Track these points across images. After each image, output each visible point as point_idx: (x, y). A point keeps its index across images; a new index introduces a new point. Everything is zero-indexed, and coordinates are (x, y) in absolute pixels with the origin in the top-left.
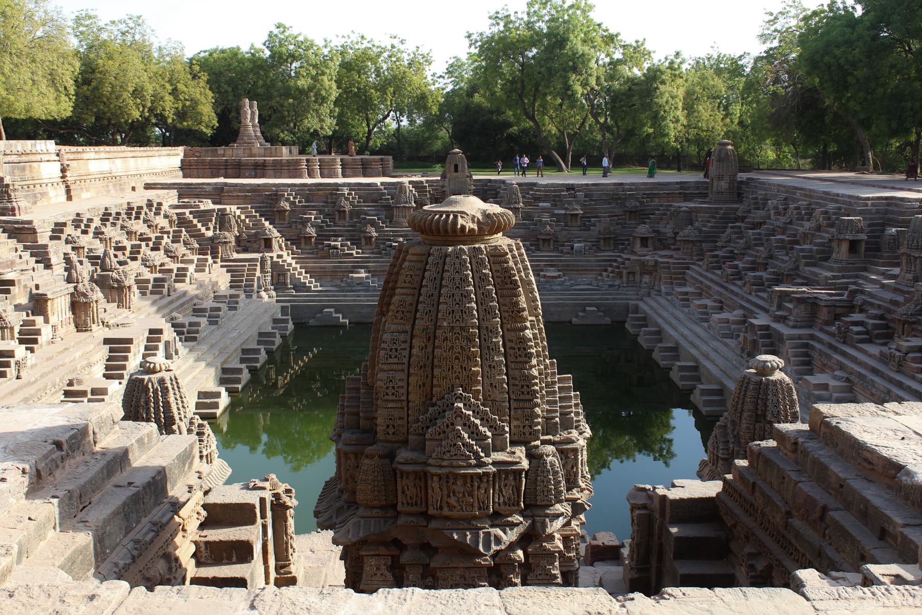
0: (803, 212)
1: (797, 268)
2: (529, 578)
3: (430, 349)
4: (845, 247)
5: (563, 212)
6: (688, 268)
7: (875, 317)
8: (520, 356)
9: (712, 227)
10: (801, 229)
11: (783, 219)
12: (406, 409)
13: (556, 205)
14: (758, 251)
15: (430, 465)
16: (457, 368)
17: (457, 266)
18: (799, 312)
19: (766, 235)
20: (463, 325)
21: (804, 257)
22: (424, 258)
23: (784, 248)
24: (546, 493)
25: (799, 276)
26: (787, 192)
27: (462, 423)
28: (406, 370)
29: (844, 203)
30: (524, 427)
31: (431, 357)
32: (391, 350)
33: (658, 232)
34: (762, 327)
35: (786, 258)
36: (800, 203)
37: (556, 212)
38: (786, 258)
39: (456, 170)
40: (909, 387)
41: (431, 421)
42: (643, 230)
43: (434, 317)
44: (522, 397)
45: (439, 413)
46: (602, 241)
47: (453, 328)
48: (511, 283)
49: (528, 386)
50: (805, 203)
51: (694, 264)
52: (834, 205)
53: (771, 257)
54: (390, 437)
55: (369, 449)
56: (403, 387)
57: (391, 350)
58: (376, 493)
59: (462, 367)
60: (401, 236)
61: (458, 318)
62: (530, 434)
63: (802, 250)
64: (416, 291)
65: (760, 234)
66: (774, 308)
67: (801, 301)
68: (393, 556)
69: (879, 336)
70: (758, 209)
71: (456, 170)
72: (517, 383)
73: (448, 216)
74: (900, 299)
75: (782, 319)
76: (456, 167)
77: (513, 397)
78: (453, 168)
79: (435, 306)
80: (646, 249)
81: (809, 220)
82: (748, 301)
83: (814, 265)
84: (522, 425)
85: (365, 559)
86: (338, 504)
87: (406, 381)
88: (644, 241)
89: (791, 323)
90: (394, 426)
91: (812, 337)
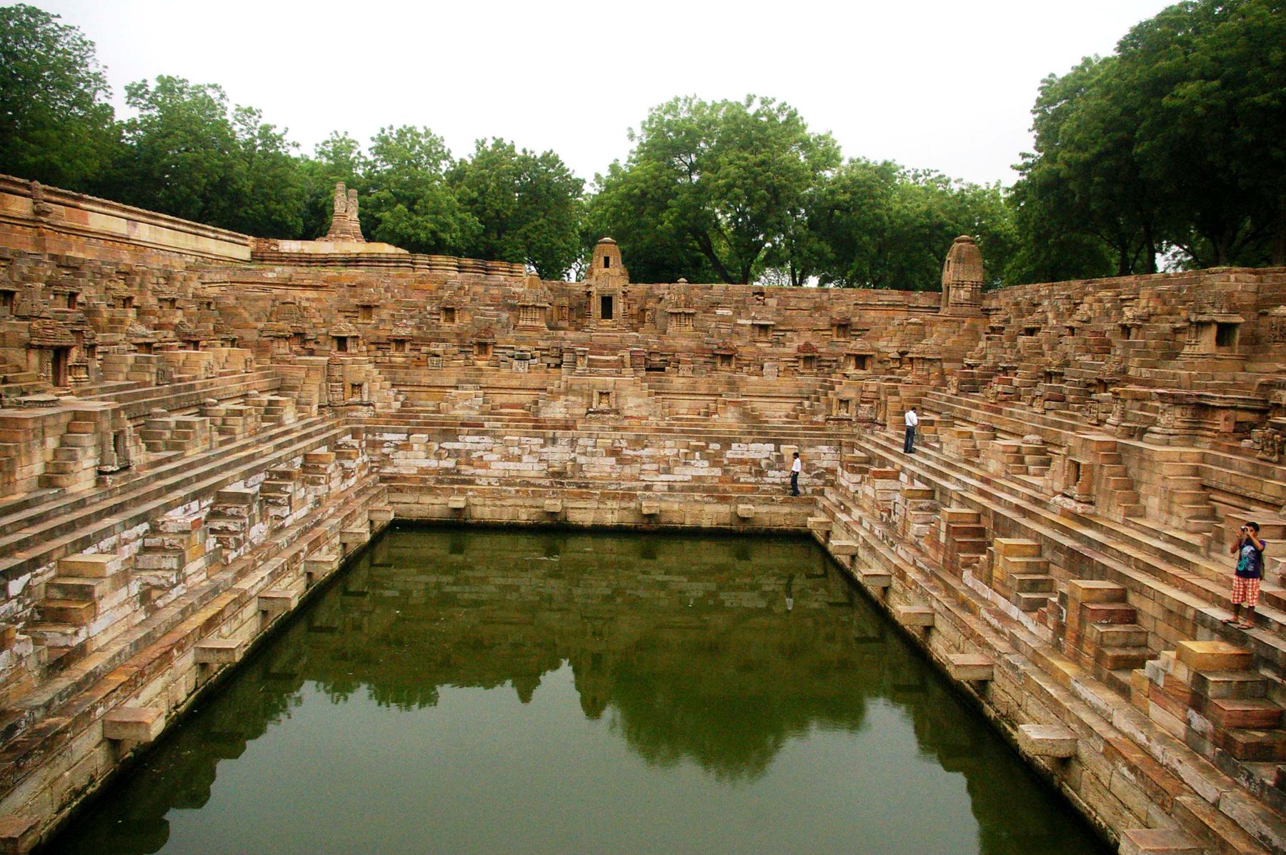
1: (1125, 371)
4: (1209, 336)
5: (750, 322)
37: (739, 322)
39: (607, 265)
42: (857, 345)
46: (801, 362)
53: (1067, 364)
71: (607, 265)
76: (607, 260)
80: (862, 372)
88: (861, 361)
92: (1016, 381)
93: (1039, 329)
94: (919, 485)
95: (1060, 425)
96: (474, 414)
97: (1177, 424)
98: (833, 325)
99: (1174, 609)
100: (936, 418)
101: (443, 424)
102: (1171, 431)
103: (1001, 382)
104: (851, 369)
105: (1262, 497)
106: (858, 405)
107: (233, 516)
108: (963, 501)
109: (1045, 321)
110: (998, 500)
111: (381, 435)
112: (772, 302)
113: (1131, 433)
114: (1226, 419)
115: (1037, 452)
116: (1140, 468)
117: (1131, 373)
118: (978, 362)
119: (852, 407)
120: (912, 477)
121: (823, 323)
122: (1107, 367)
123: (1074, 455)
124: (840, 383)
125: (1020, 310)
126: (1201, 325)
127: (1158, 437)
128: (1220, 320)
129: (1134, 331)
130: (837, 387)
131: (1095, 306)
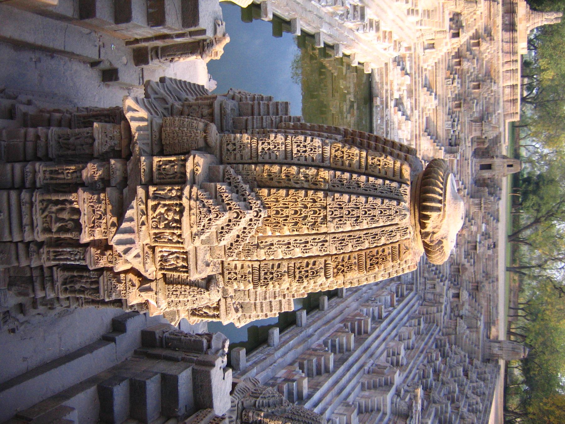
0: (474, 407)
1: (434, 402)
2: (109, 273)
3: (306, 185)
5: (478, 240)
8: (300, 272)
9: (466, 342)
10: (462, 406)
11: (469, 392)
12: (250, 161)
13: (483, 235)
14: (448, 373)
15: (191, 188)
16: (286, 212)
17: (388, 212)
18: (403, 406)
19: (459, 380)
20: (329, 219)
21: (442, 408)
22: (397, 178)
23: (449, 393)
24: (175, 293)
25: (429, 404)
26: (489, 394)
27: (231, 218)
28: (285, 161)
30: (236, 273)
31: (297, 186)
32: (305, 146)
33: (463, 305)
35: (442, 394)
37: (478, 236)
38: (442, 394)
41: (236, 187)
43: (337, 189)
44: (262, 273)
45: (243, 195)
46: (457, 267)
47: (325, 208)
48: (371, 265)
49: (272, 278)
50: (481, 408)
53: (443, 383)
54: (225, 146)
55: (213, 128)
56: (270, 158)
57: (305, 146)
58: (171, 135)
59: (288, 216)
60: (461, 128)
61: (335, 213)
62: (229, 279)
63: (447, 406)
64: (364, 170)
66: (406, 387)
67: (410, 407)
68: (120, 151)
70: (478, 374)
72: (275, 269)
73: (440, 202)
75: (398, 393)
77: (262, 264)
78: (511, 163)
79: (347, 190)
80: (451, 296)
81: (469, 411)
82: (412, 368)
83: (436, 415)
84: (237, 271)
85: (118, 126)
86: (170, 100)
87: (276, 161)
88: (457, 296)
89: (395, 400)
90: (234, 150)
91: (385, 414)
96: (422, 105)
98: (478, 283)
101: (416, 90)
104: (452, 292)
106: (433, 293)
107: (354, 15)
111: (409, 60)
112: (490, 252)
115: (398, 362)
119: (432, 290)
121: (479, 277)
124: (444, 285)
125: (481, 374)
130: (442, 283)
131: (475, 401)
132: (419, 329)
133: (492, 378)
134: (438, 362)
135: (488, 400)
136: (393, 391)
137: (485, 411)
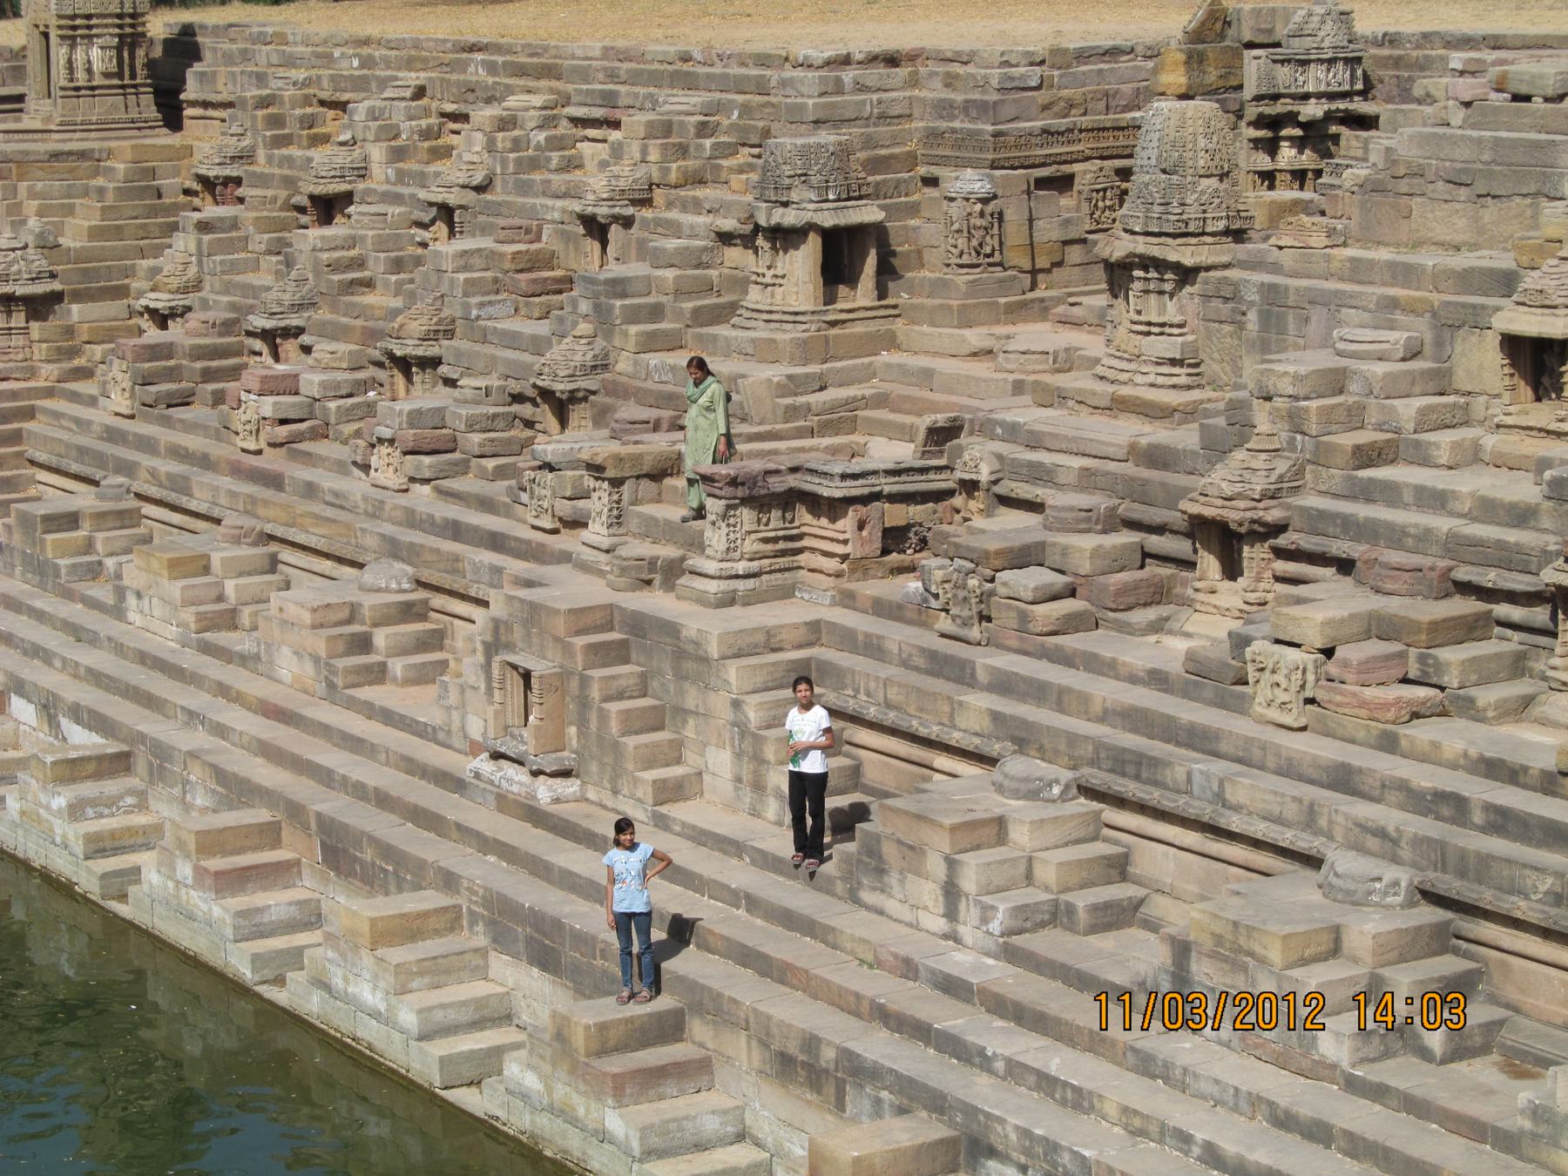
1: (601, 365)
4: (804, 262)
6: (30, 414)
7: (1088, 521)
9: (95, 233)
26: (410, 64)
29: (740, 86)
34: (587, 619)
36: (513, 101)
40: (1403, 786)
50: (537, 100)
51: (49, 393)
52: (696, 99)
65: (352, 242)
69: (1132, 599)
74: (1186, 437)
92: (312, 382)
93: (348, 198)
94: (82, 739)
95: (456, 531)
97: (751, 546)
99: (793, 1048)
100: (84, 499)
102: (741, 567)
103: (270, 387)
105: (955, 738)
108: (236, 790)
109: (362, 173)
110: (324, 776)
113: (647, 575)
114: (861, 526)
115: (409, 612)
116: (680, 676)
117: (623, 364)
118: (180, 301)
120: (49, 708)
122: (562, 362)
123: (510, 647)
125: (276, 121)
126: (785, 237)
127: (712, 586)
128: (828, 220)
129: (615, 232)
132: (100, 516)
133: (290, 62)
134: (312, 382)
135: (462, 66)
136: (656, 602)
137: (550, 72)
